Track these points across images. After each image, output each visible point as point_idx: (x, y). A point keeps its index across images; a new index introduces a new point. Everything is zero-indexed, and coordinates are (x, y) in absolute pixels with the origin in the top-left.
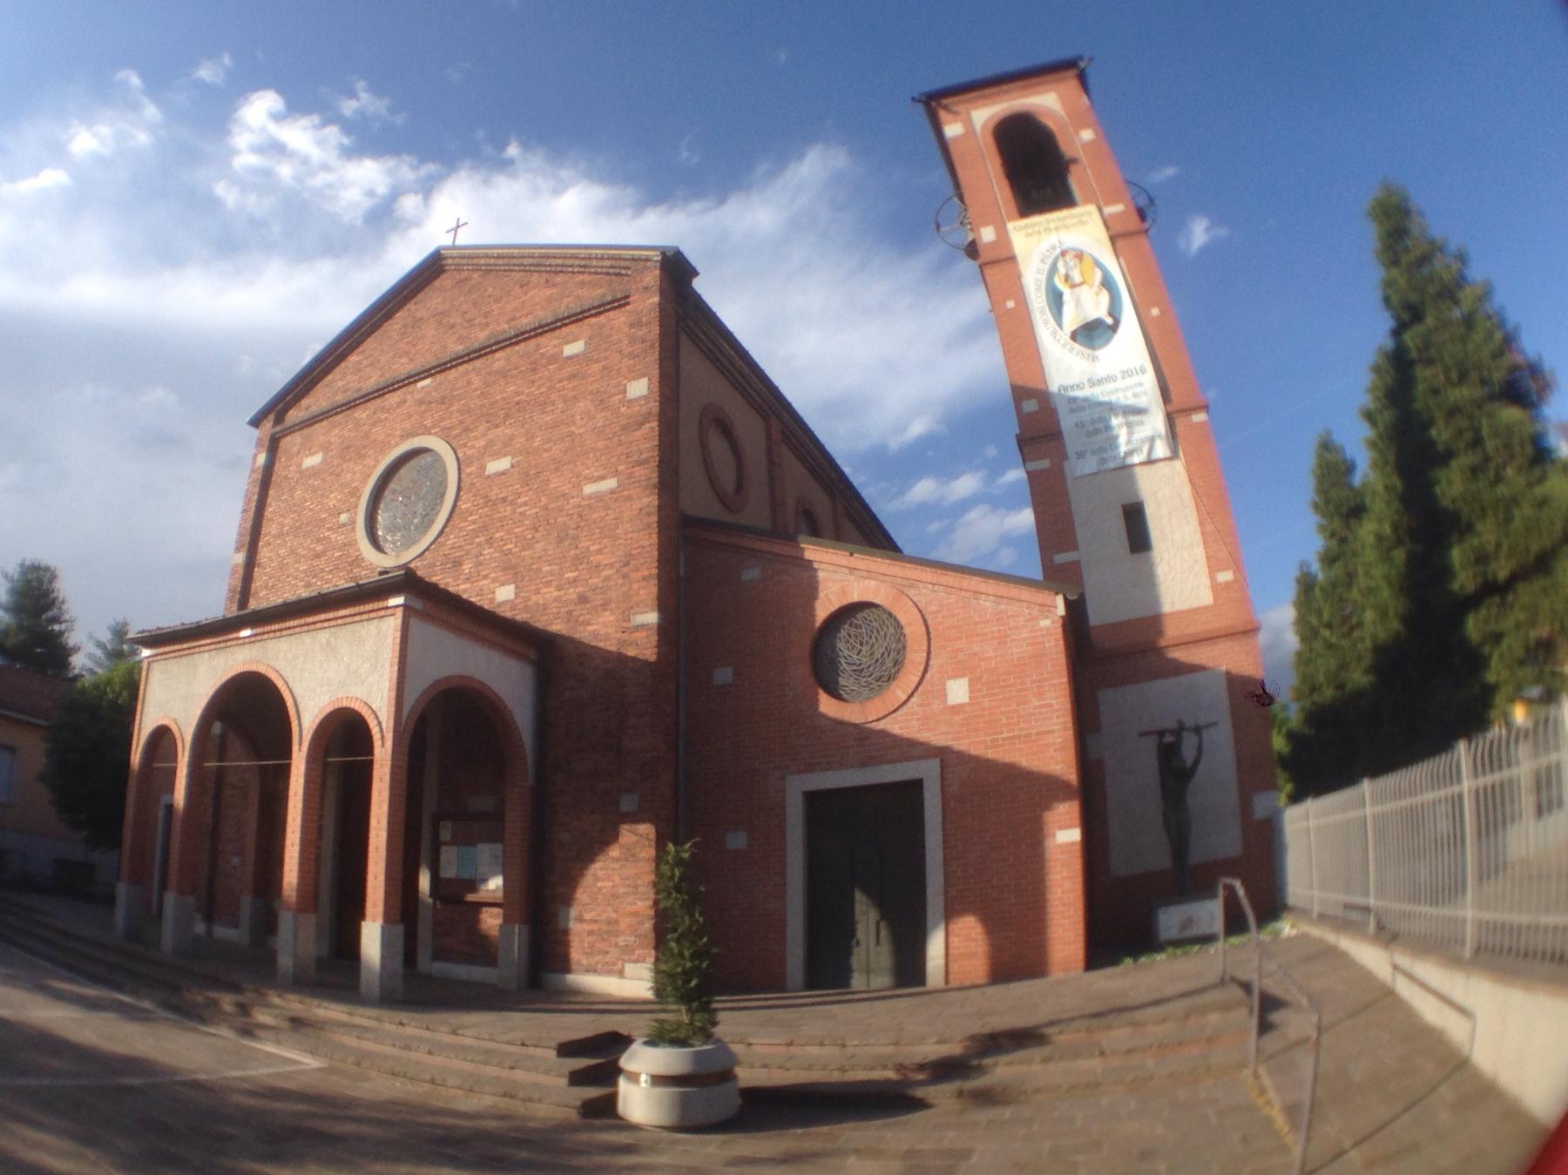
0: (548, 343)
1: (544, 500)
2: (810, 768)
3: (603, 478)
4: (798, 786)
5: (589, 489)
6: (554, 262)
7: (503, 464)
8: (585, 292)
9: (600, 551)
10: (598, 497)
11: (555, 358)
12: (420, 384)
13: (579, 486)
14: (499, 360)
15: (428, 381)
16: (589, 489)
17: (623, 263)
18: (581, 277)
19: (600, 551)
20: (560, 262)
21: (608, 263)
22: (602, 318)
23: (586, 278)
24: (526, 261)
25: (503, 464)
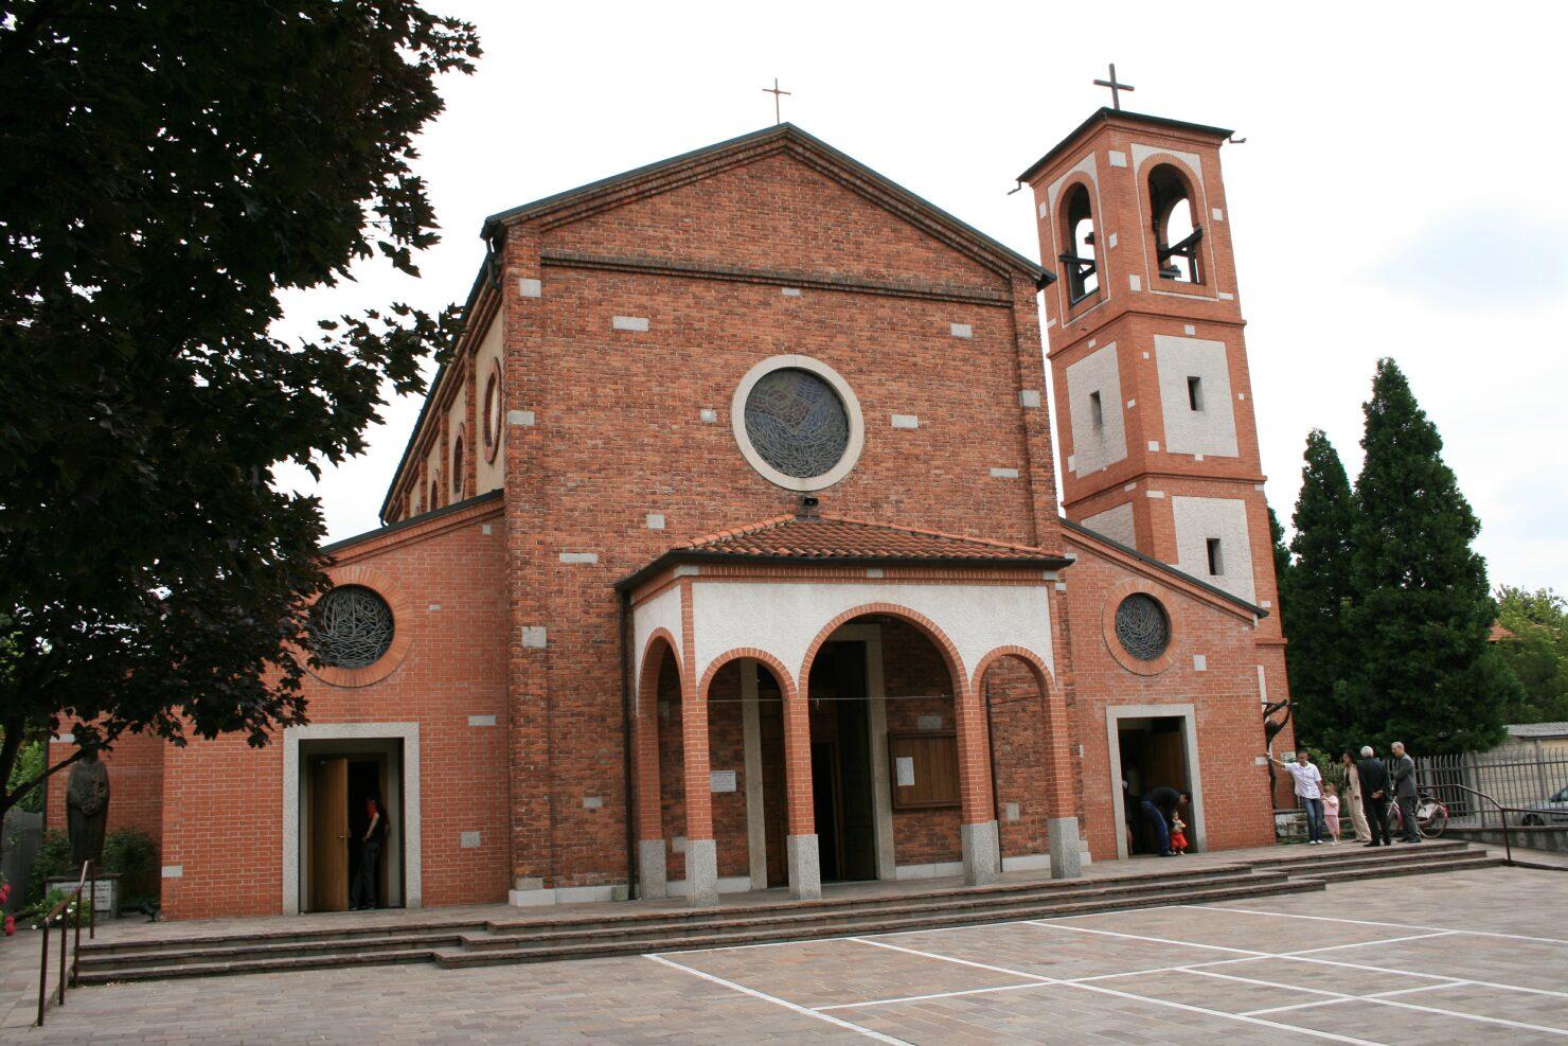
0: (936, 315)
1: (957, 470)
2: (1120, 702)
3: (1004, 466)
4: (1115, 713)
5: (996, 472)
6: (934, 226)
7: (911, 422)
8: (962, 272)
9: (1011, 526)
10: (1004, 480)
11: (944, 333)
12: (786, 291)
13: (986, 464)
14: (885, 308)
15: (796, 292)
16: (996, 472)
17: (1003, 265)
18: (955, 254)
19: (1011, 526)
20: (939, 228)
21: (991, 258)
22: (983, 311)
23: (963, 260)
24: (900, 206)
25: (911, 422)
